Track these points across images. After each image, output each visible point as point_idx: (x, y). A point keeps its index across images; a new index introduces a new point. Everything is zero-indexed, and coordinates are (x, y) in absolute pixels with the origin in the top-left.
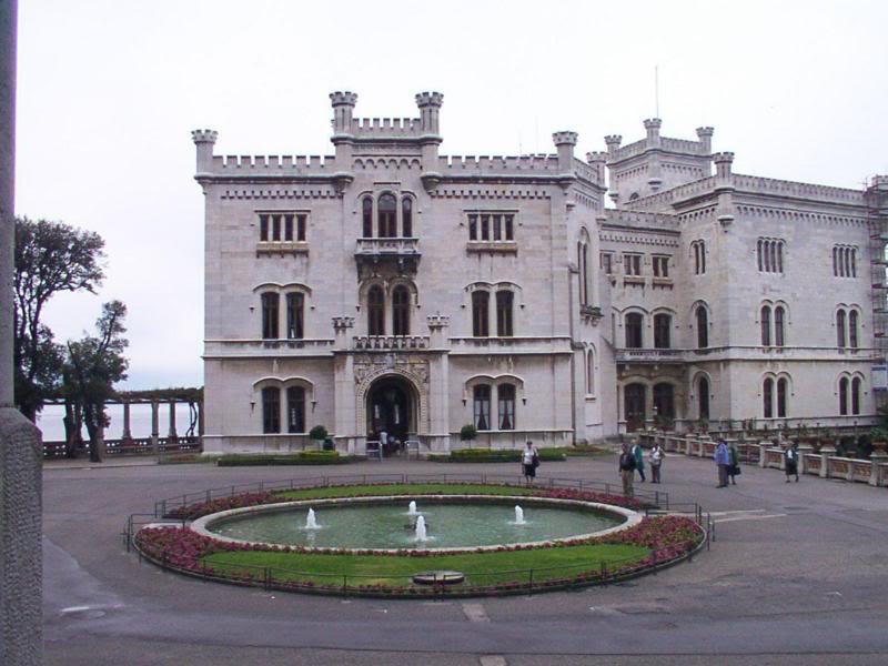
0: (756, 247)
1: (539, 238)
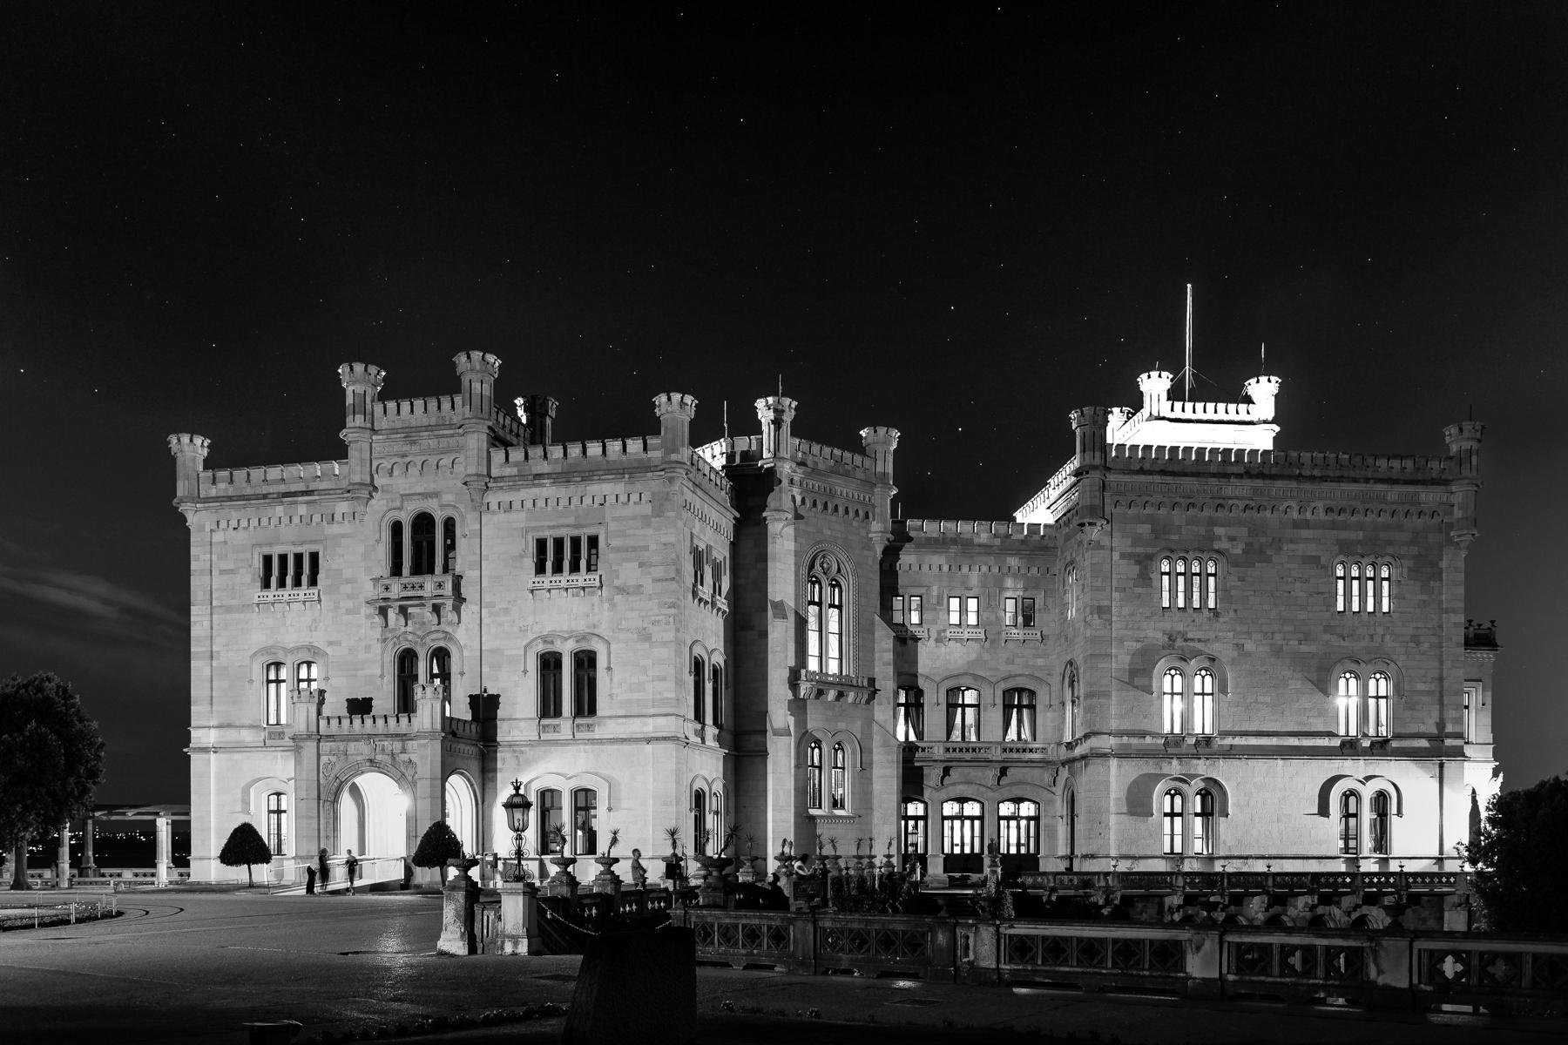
1: (636, 565)
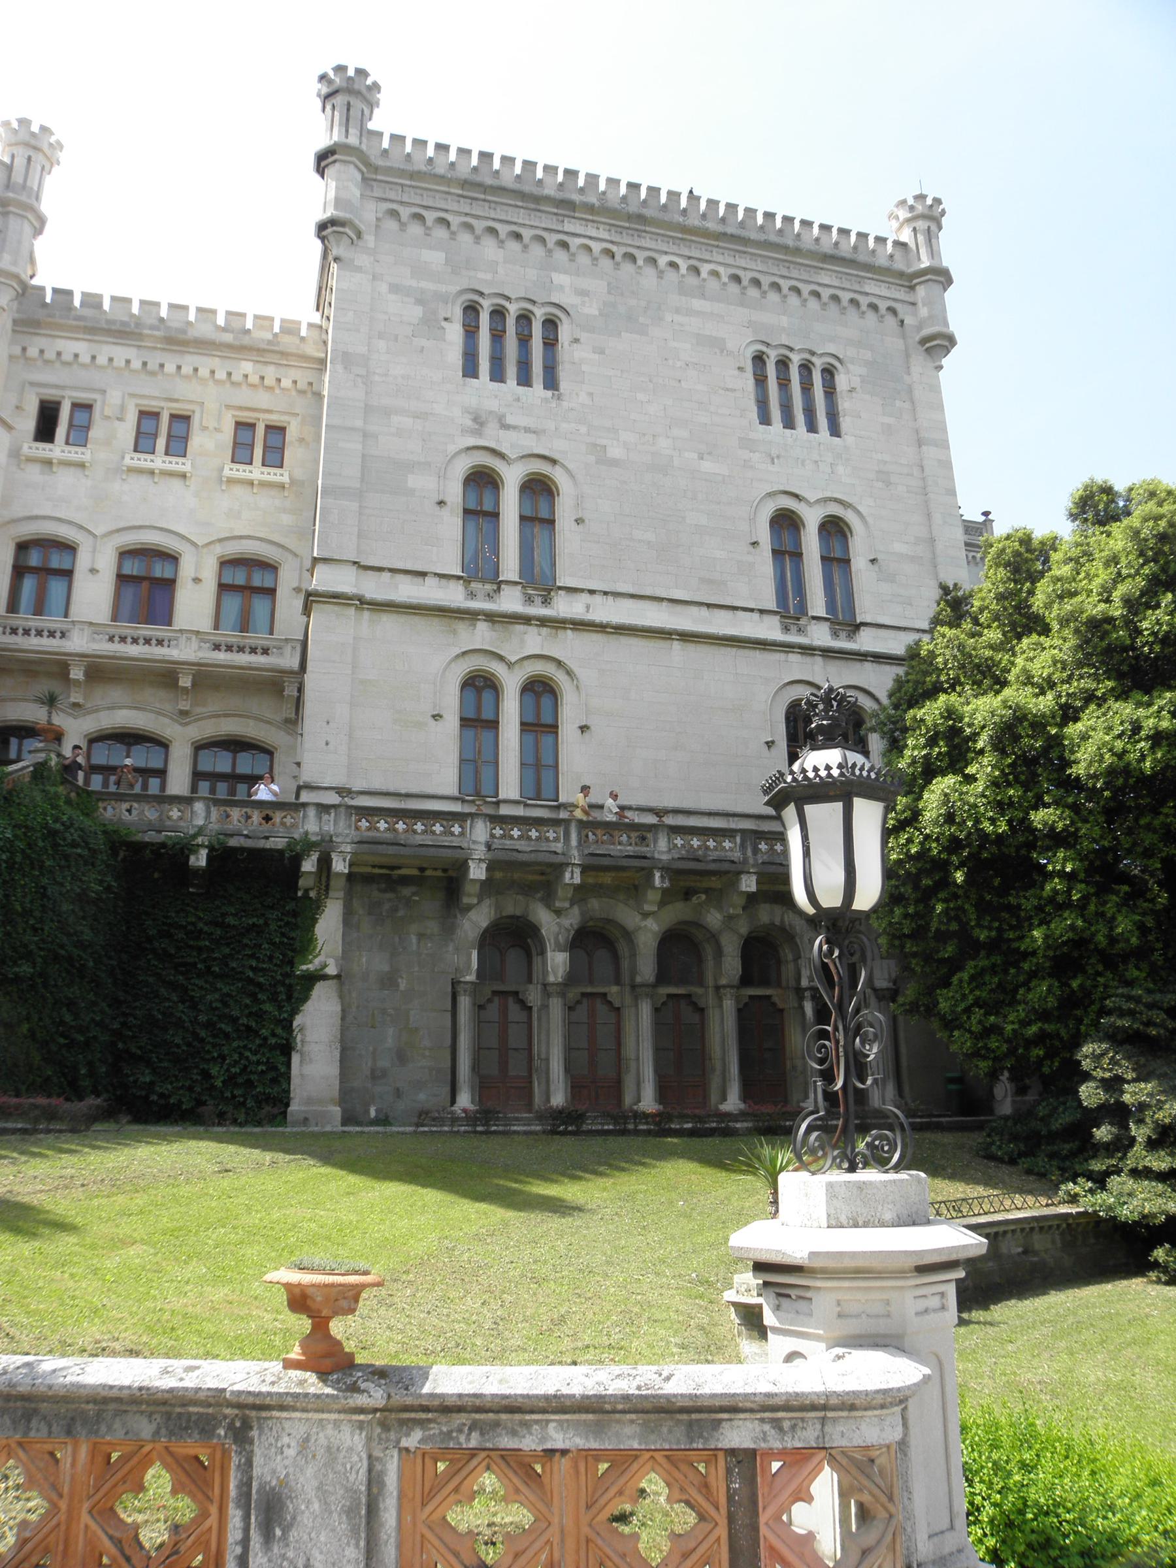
0: (458, 313)
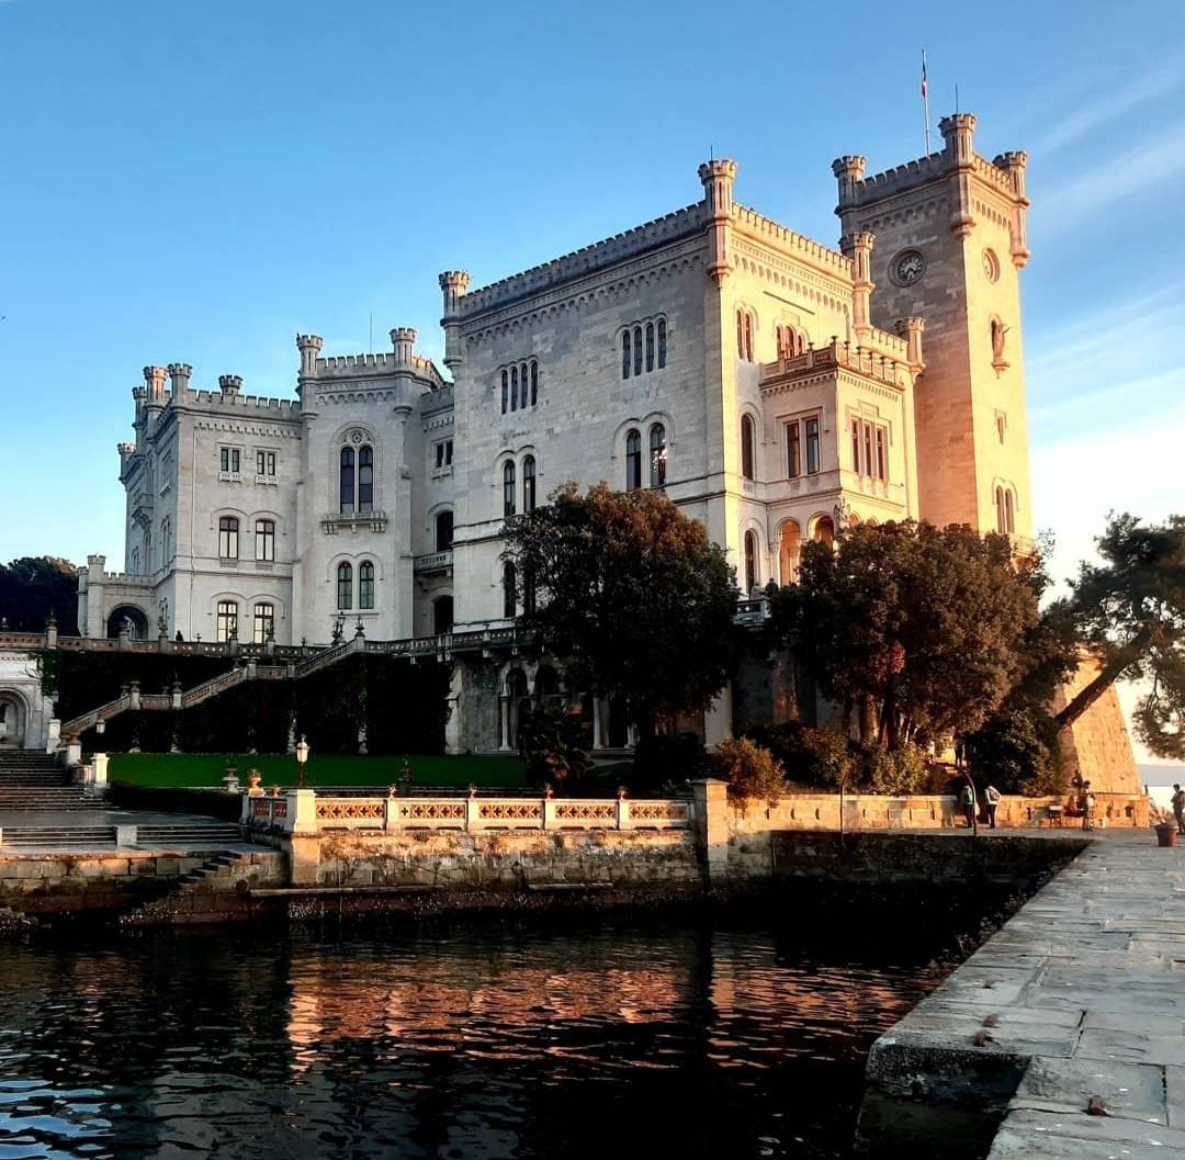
0: (499, 380)
